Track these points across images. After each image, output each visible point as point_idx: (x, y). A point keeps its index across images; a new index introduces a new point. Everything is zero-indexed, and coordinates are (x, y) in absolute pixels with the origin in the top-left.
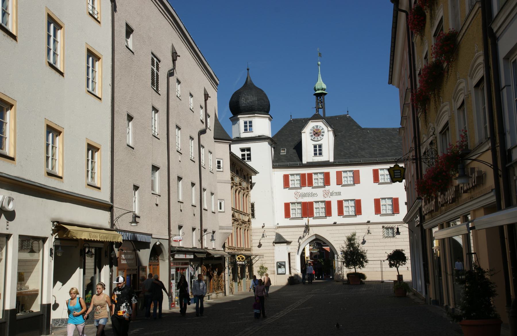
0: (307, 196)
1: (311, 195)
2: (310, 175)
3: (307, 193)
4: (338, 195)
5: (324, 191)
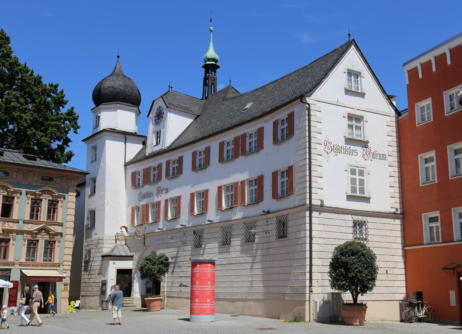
3: (342, 147)
4: (382, 159)
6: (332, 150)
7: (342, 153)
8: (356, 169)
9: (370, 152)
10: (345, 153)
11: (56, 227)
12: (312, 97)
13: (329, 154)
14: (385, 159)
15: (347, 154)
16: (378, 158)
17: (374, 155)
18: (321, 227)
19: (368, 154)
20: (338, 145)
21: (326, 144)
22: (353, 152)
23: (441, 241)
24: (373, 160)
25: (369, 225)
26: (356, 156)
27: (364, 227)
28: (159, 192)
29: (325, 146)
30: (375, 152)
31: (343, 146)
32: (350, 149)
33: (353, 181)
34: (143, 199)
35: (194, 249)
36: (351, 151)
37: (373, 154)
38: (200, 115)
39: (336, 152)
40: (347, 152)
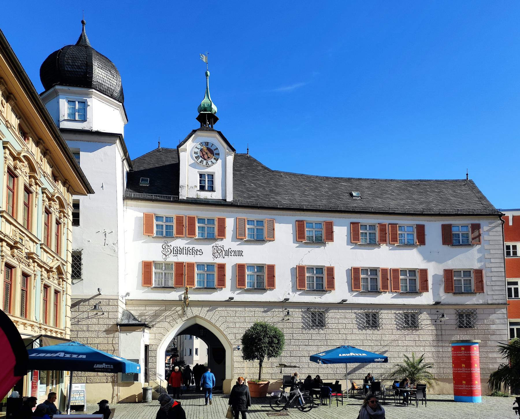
0: (184, 253)
1: (191, 251)
2: (191, 220)
3: (184, 248)
4: (237, 255)
5: (215, 248)
6: (171, 251)
7: (183, 254)
9: (222, 250)
10: (187, 253)
15: (190, 254)
16: (233, 254)
21: (164, 247)
24: (226, 257)
26: (201, 255)
29: (164, 249)
30: (229, 249)
31: (185, 248)
32: (194, 249)
36: (195, 252)
37: (226, 251)
39: (177, 253)
40: (190, 252)
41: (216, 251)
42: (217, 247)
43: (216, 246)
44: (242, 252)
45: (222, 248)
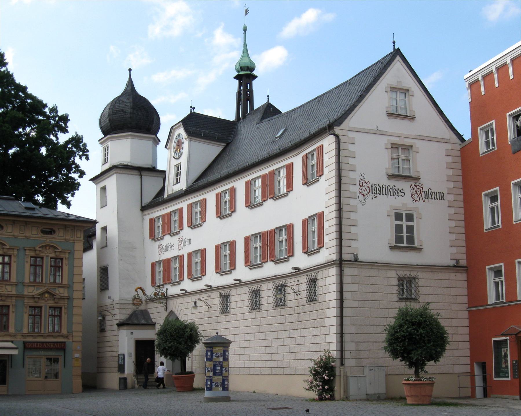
0: (384, 193)
1: (391, 191)
3: (384, 186)
4: (438, 198)
5: (414, 187)
6: (370, 191)
7: (383, 194)
8: (401, 214)
9: (422, 191)
10: (387, 193)
11: (61, 290)
12: (343, 126)
13: (366, 197)
14: (442, 198)
15: (391, 195)
16: (433, 197)
17: (428, 195)
18: (355, 288)
19: (419, 193)
20: (377, 185)
21: (361, 185)
22: (398, 191)
23: (504, 301)
24: (426, 200)
25: (421, 283)
26: (403, 196)
27: (413, 286)
28: (181, 243)
29: (361, 186)
31: (385, 186)
32: (395, 189)
33: (399, 229)
34: (164, 253)
35: (221, 315)
36: (396, 192)
38: (230, 142)
39: (376, 193)
40: (391, 193)
41: (415, 192)
42: (416, 186)
43: (414, 185)
44: (444, 194)
45: (421, 187)
